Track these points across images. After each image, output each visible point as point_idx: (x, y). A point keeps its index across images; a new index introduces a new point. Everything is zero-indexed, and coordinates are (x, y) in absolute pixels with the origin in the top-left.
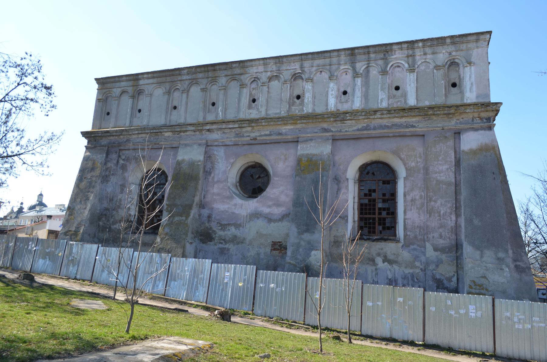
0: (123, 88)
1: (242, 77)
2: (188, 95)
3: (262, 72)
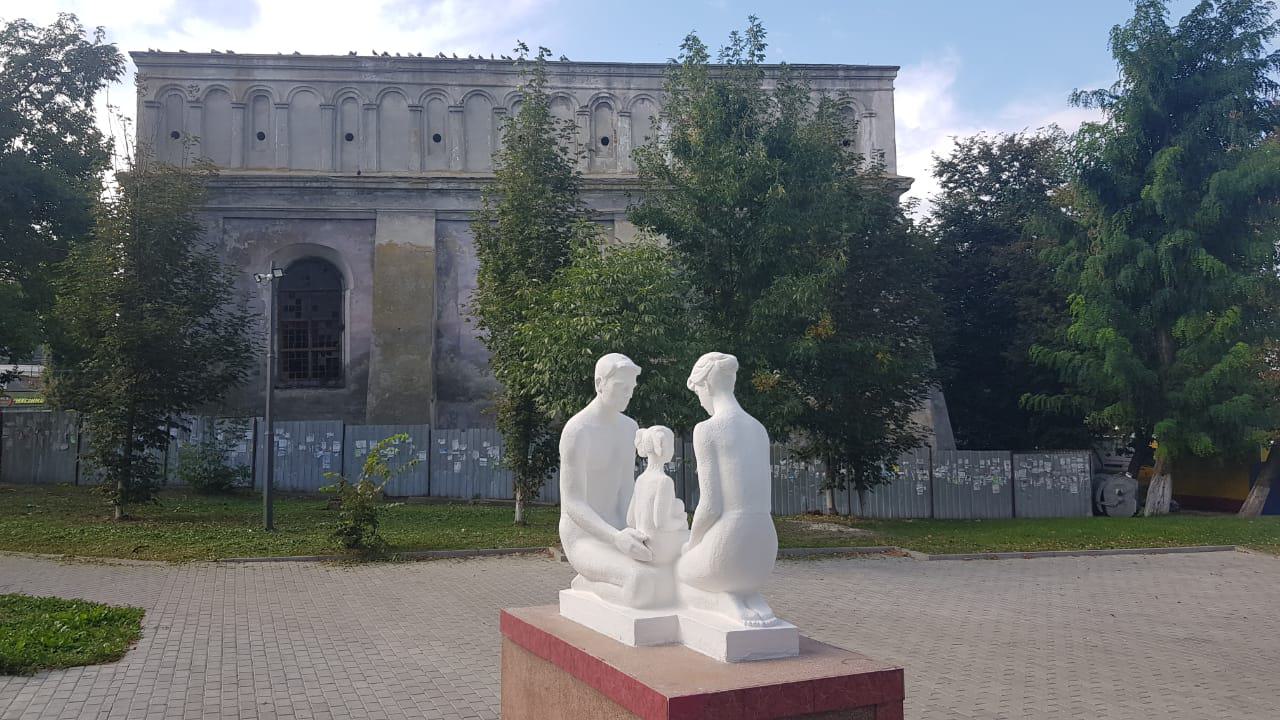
0: (210, 83)
1: (495, 92)
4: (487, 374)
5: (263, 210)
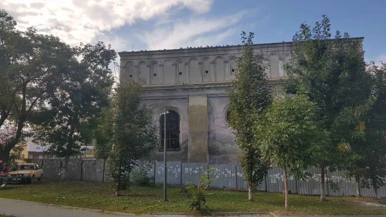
2: (189, 66)
3: (237, 54)
4: (225, 146)
5: (156, 97)
